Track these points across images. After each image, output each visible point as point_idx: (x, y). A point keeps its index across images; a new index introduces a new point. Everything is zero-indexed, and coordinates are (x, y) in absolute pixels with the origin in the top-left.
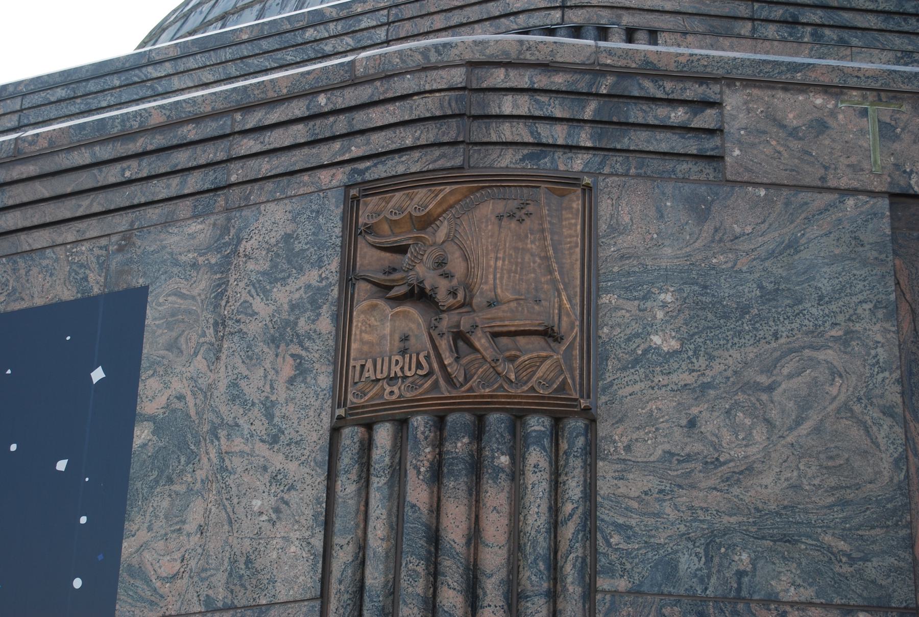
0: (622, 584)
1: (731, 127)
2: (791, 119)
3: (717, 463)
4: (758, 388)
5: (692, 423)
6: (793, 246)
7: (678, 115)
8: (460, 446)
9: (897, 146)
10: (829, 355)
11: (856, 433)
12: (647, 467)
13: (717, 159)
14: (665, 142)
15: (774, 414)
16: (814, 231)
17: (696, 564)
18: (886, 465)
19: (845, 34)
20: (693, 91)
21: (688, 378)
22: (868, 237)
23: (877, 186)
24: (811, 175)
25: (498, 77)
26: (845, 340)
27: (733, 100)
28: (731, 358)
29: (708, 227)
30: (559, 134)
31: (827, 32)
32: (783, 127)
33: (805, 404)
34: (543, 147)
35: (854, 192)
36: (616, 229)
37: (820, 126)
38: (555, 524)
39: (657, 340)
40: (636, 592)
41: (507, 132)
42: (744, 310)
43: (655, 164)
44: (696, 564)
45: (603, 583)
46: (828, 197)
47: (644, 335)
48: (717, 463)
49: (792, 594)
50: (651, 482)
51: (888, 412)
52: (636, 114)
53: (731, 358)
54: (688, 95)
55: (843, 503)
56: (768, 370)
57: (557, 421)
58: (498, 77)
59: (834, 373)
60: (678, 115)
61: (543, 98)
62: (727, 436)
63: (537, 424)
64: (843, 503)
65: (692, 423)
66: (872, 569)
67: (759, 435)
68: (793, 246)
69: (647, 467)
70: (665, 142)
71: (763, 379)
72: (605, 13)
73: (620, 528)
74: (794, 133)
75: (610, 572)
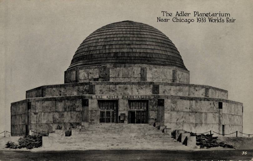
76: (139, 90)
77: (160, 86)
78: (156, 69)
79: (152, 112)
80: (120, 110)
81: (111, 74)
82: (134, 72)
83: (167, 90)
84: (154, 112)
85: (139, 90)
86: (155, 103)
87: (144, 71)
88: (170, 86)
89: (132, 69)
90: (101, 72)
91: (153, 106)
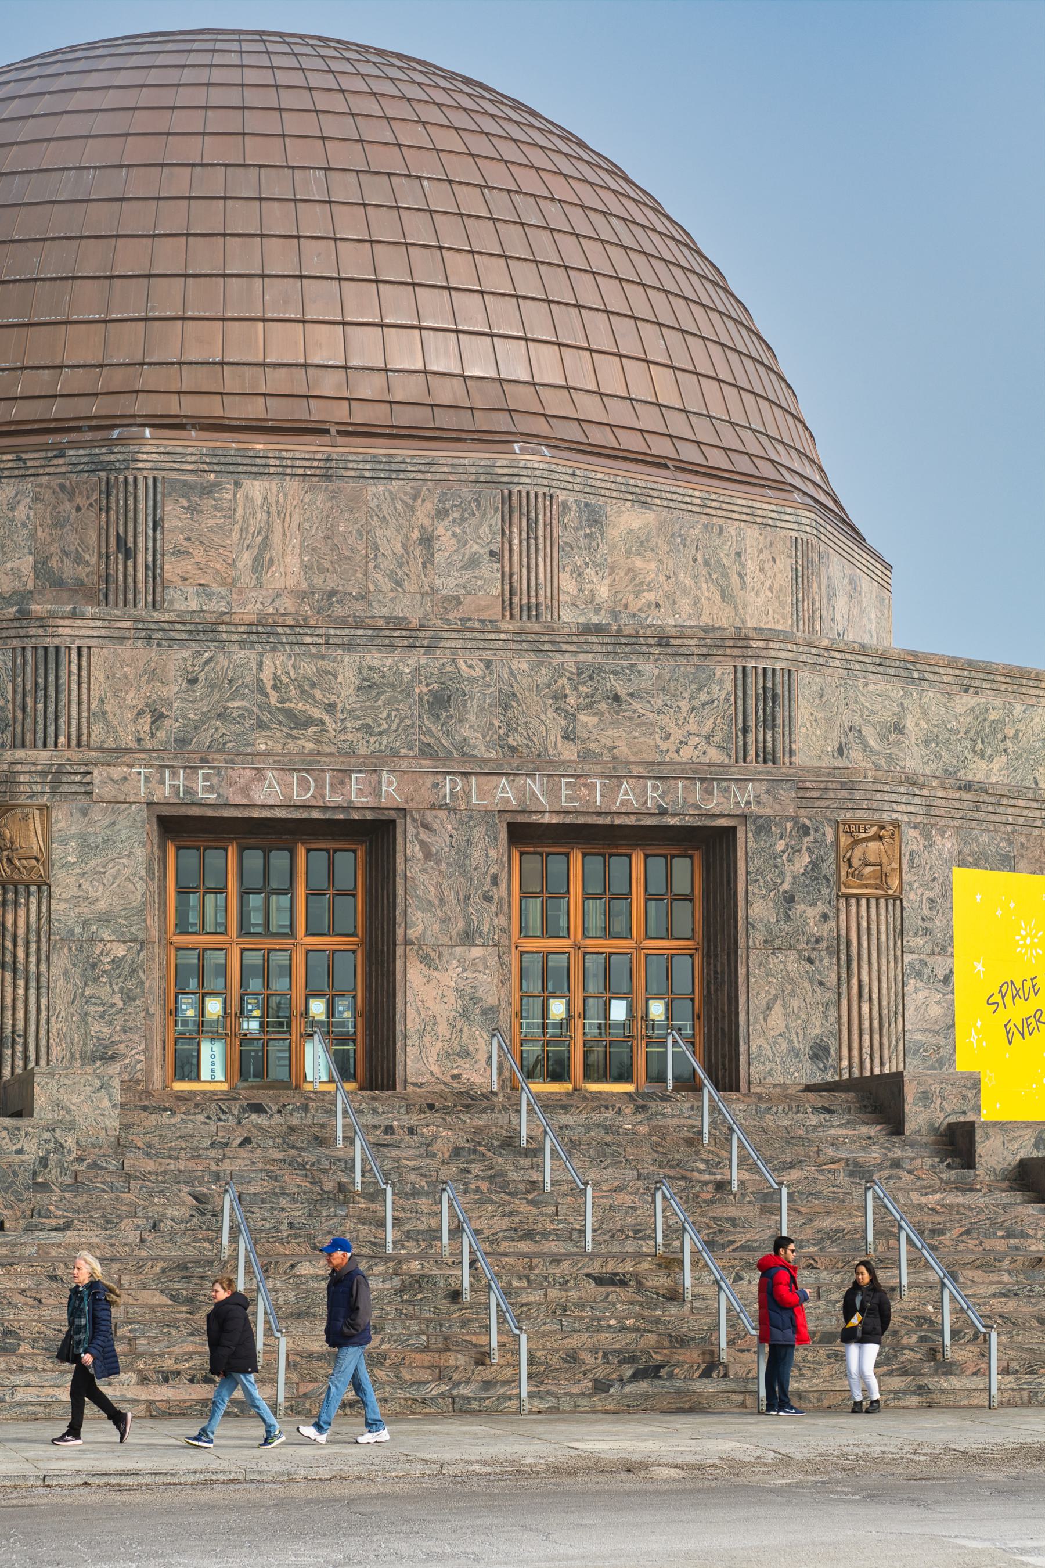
0: (58, 937)
1: (97, 780)
2: (115, 777)
3: (87, 898)
4: (101, 873)
5: (80, 886)
6: (114, 823)
7: (78, 778)
8: (10, 896)
9: (150, 785)
10: (123, 861)
11: (131, 886)
12: (66, 901)
13: (90, 793)
14: (74, 788)
15: (105, 881)
16: (121, 817)
17: (80, 930)
18: (139, 896)
19: (171, 643)
20: (83, 769)
21: (79, 871)
22: (138, 819)
23: (143, 800)
24: (121, 798)
25: (18, 768)
26: (129, 856)
27: (96, 772)
28: (93, 863)
29: (87, 818)
30: (38, 788)
31: (164, 642)
32: (112, 780)
33: (115, 878)
34: (34, 794)
35: (135, 803)
36: (57, 821)
37: (125, 779)
38: (39, 919)
39: (69, 858)
40: (62, 939)
41: (22, 788)
42: (98, 847)
43: (70, 797)
44: (80, 930)
45: (52, 937)
46: (126, 805)
47: (65, 857)
48: (87, 898)
49: (108, 938)
50: (67, 905)
51: (141, 878)
52: (64, 779)
53: (93, 863)
54: (82, 770)
55: (125, 909)
56: (104, 867)
57: (39, 887)
58: (18, 768)
59: (125, 866)
60: (78, 778)
61: (34, 775)
62: (90, 889)
63: (33, 889)
64: (125, 909)
65: (80, 886)
66: (132, 929)
67: (101, 888)
68: (114, 823)
69: (66, 901)
70: (74, 788)
71: (103, 870)
72: (68, 639)
73: (57, 920)
74: (115, 782)
75: (54, 934)
76: (583, 717)
77: (803, 676)
78: (650, 517)
79: (775, 963)
80: (413, 933)
81: (178, 553)
82: (427, 540)
83: (868, 732)
84: (792, 964)
85: (583, 717)
86: (804, 859)
87: (532, 526)
88: (897, 694)
89: (412, 509)
90: (58, 523)
91: (790, 899)
